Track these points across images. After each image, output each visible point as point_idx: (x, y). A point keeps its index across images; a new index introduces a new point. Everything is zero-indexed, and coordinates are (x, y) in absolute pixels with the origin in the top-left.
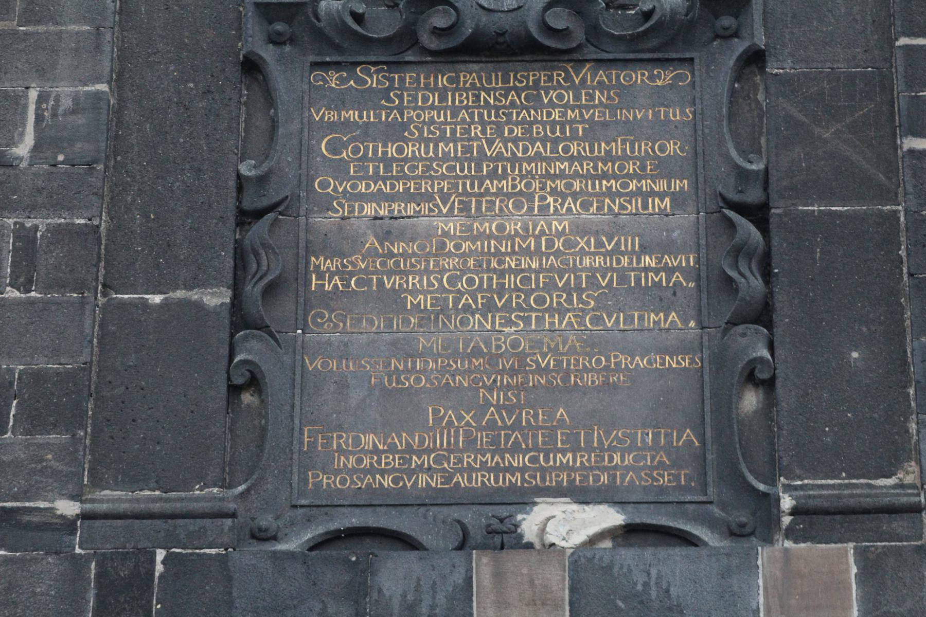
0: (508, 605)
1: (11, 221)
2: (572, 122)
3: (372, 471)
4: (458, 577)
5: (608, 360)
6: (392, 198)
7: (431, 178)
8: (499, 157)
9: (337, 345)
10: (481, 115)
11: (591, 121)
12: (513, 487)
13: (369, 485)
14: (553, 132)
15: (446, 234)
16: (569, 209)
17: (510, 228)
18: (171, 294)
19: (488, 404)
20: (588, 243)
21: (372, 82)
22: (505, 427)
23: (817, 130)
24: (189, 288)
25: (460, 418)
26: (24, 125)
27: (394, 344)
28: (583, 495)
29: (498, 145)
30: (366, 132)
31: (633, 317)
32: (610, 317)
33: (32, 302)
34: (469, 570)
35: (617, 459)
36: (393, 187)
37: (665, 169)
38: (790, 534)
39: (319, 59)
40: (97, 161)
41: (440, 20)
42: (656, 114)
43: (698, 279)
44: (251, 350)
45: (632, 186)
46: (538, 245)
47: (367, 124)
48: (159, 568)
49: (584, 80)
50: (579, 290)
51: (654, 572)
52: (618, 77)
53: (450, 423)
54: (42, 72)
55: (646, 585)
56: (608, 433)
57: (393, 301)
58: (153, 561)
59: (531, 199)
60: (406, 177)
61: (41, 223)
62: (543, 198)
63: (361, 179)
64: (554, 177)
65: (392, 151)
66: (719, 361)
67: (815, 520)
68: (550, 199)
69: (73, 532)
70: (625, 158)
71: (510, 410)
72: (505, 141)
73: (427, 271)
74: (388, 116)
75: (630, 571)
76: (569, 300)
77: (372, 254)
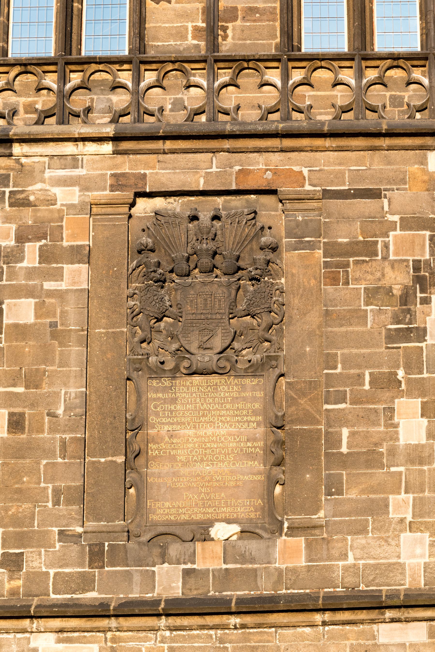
0: (206, 558)
1: (58, 436)
2: (227, 397)
3: (167, 514)
4: (192, 550)
5: (237, 477)
6: (172, 424)
7: (184, 417)
8: (205, 410)
9: (157, 471)
10: (199, 395)
11: (233, 397)
12: (209, 519)
13: (167, 519)
14: (221, 401)
15: (189, 436)
16: (226, 427)
17: (208, 434)
18: (107, 459)
19: (202, 492)
20: (231, 438)
21: (167, 383)
22: (207, 500)
23: (300, 401)
24: (113, 456)
25: (193, 497)
26: (61, 403)
27: (174, 473)
28: (229, 522)
29: (205, 405)
30: (165, 401)
31: (244, 463)
32: (237, 463)
33: (65, 463)
34: (195, 548)
35: (239, 509)
36: (173, 420)
37: (255, 413)
38: (286, 535)
39: (150, 376)
40: (83, 415)
41: (186, 364)
42: (252, 394)
43: (264, 451)
44: (131, 476)
45: (245, 419)
46: (216, 439)
47: (165, 398)
48: (106, 548)
49: (231, 383)
50: (229, 454)
51: (247, 547)
52: (241, 381)
53: (190, 499)
54: (65, 385)
55: (245, 551)
56: (236, 501)
57: (173, 459)
58: (104, 546)
59: (214, 423)
60: (177, 417)
61: (67, 436)
62: (218, 423)
63: (164, 417)
64: (221, 416)
65: (173, 408)
66: (269, 477)
67: (294, 530)
68: (220, 424)
69: (81, 537)
70: (243, 409)
71: (208, 494)
72: (207, 404)
73: (184, 449)
74: (171, 395)
75: (240, 547)
76: (226, 458)
77: (167, 443)
